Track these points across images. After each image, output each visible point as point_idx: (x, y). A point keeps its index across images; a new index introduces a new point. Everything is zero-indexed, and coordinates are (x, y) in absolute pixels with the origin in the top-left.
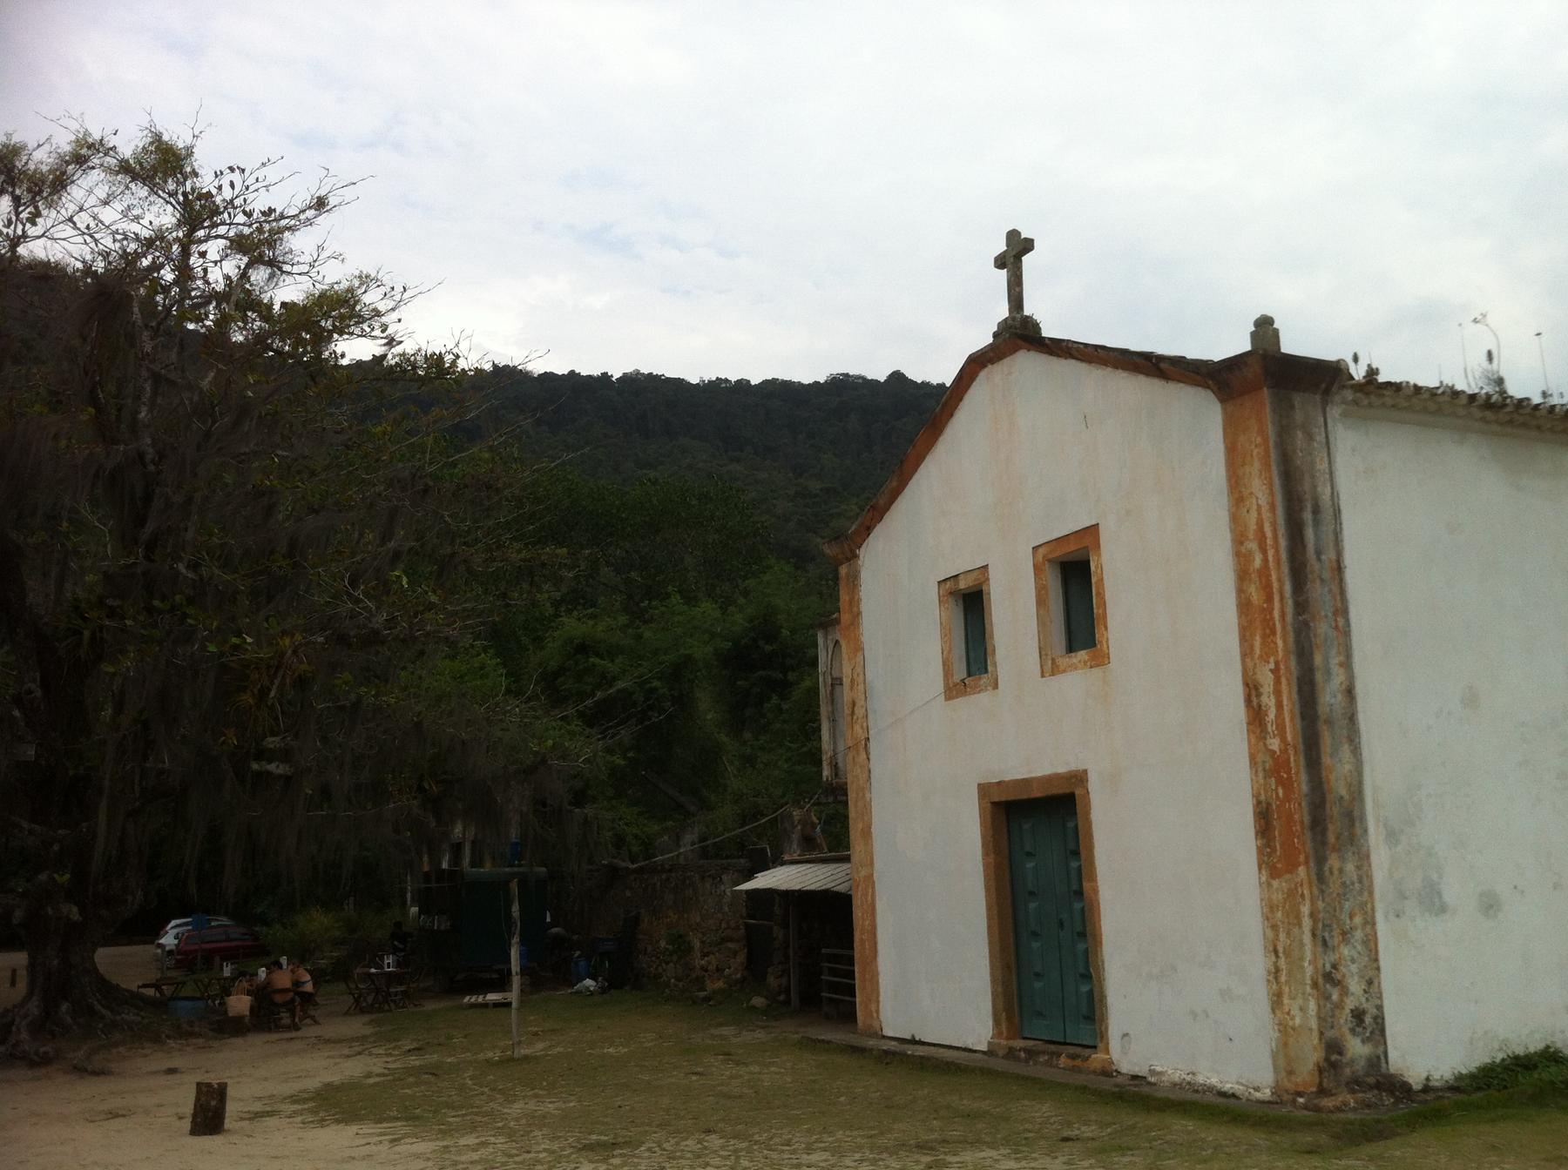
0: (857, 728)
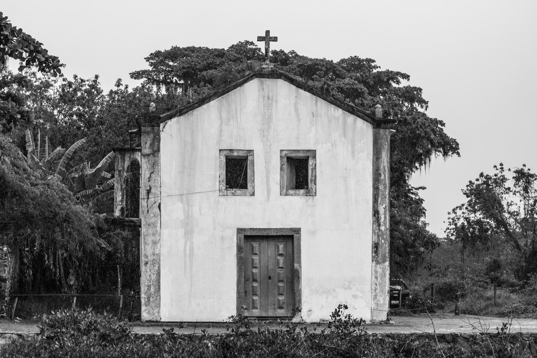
0: (152, 200)
